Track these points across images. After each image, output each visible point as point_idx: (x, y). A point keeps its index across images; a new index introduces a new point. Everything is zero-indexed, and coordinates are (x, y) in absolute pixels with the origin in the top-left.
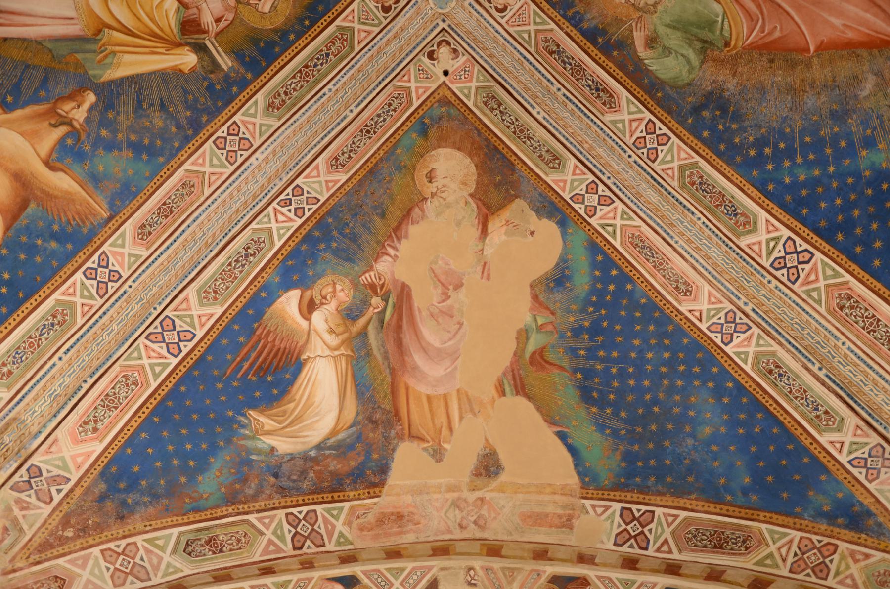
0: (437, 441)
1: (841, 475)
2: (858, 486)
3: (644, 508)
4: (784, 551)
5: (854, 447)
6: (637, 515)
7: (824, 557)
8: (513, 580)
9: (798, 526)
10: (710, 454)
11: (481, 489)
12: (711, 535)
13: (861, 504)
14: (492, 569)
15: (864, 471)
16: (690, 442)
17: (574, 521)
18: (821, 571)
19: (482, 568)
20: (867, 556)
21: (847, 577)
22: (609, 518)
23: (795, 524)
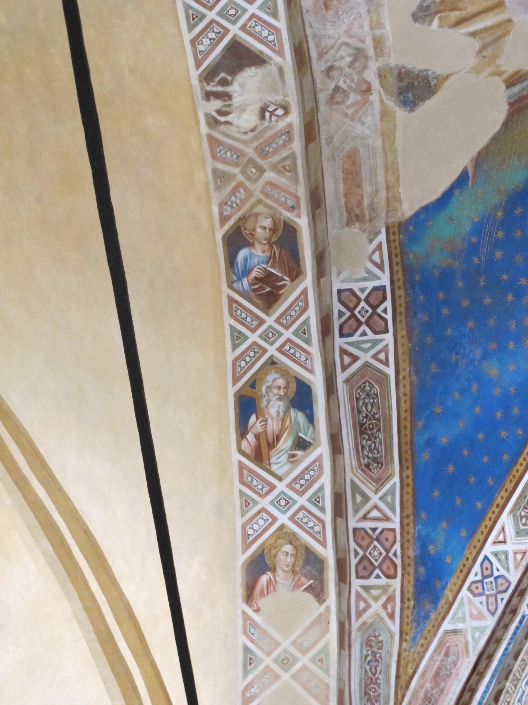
0: (441, 8)
1: (469, 553)
2: (462, 578)
3: (389, 317)
4: (375, 514)
5: (503, 557)
6: (379, 310)
7: (380, 567)
8: (279, 172)
9: (406, 521)
10: (466, 383)
11: (382, 86)
12: (373, 416)
13: (444, 588)
14: (290, 140)
15: (479, 577)
16: (478, 353)
17: (357, 225)
18: (365, 568)
19: (290, 126)
20: (392, 616)
21: (365, 601)
22: (369, 272)
23: (407, 516)
